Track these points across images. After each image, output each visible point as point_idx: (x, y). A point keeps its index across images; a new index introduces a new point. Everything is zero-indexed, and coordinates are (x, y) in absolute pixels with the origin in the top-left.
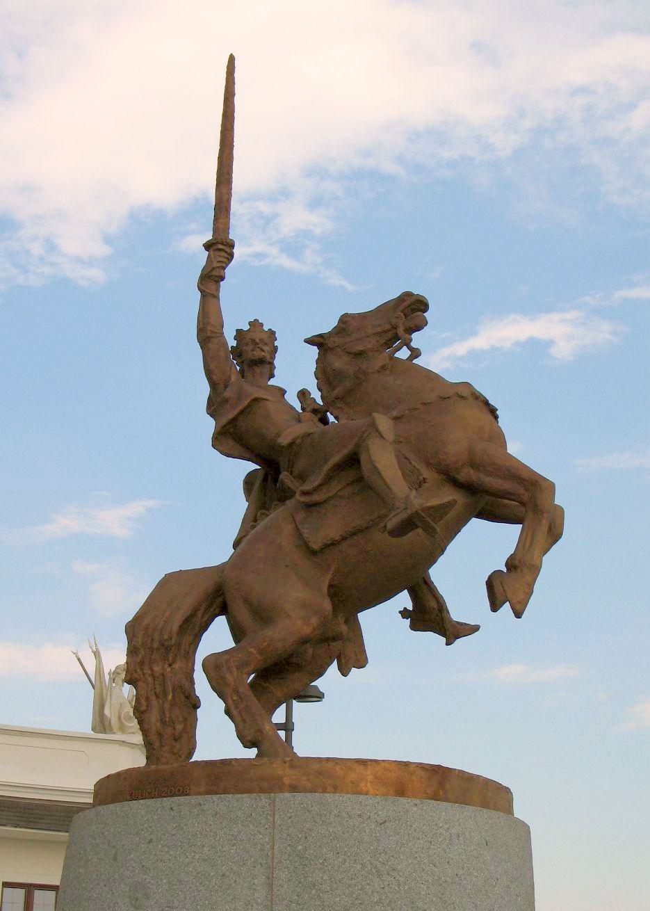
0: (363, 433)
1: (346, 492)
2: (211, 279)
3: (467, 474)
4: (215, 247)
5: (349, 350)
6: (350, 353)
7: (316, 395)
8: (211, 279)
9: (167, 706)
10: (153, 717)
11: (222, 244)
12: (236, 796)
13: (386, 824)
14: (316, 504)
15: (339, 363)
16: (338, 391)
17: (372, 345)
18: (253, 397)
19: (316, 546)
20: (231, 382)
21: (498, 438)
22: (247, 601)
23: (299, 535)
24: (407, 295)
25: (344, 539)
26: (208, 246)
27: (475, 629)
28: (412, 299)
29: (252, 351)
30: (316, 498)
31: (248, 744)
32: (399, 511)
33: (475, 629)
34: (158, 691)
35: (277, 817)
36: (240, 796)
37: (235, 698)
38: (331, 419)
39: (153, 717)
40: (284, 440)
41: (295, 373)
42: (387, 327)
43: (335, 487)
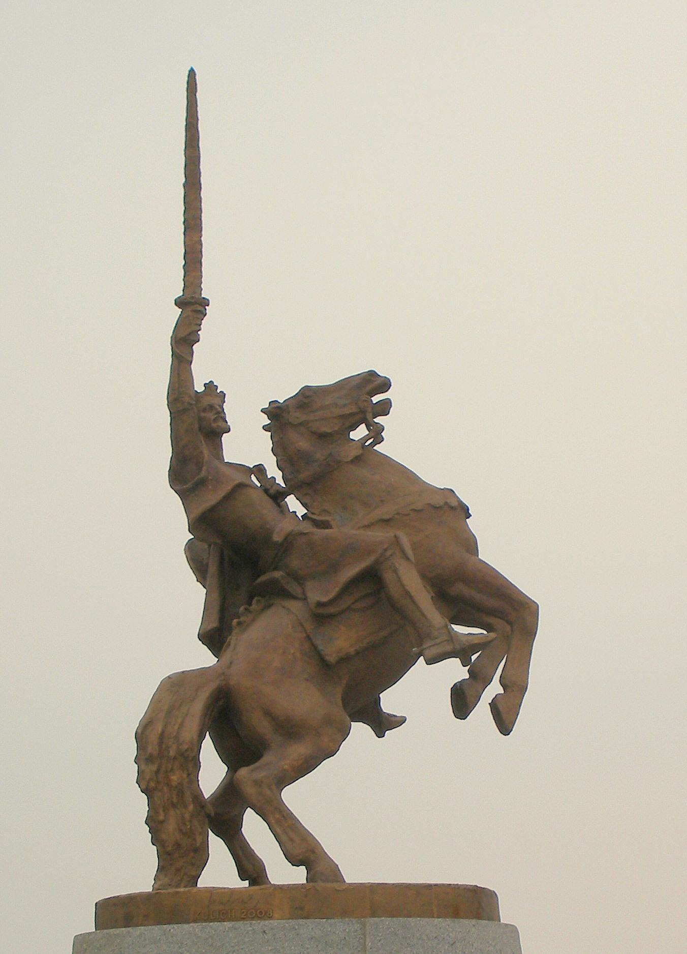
0: (385, 550)
1: (359, 605)
2: (184, 341)
3: (460, 589)
4: (194, 307)
5: (313, 430)
6: (314, 433)
7: (274, 472)
8: (184, 341)
9: (187, 816)
10: (171, 826)
11: (201, 305)
12: (329, 921)
13: (458, 944)
14: (332, 616)
15: (303, 443)
16: (304, 475)
17: (330, 426)
18: (236, 482)
19: (332, 659)
20: (205, 460)
21: (471, 545)
22: (268, 713)
23: (315, 647)
24: (372, 374)
25: (358, 653)
26: (179, 303)
27: (402, 721)
28: (379, 381)
29: (215, 420)
30: (332, 610)
31: (295, 862)
32: (438, 641)
33: (402, 721)
34: (175, 800)
35: (368, 940)
36: (333, 921)
37: (277, 816)
38: (293, 503)
39: (171, 826)
40: (277, 538)
41: (248, 444)
42: (354, 409)
43: (347, 602)
